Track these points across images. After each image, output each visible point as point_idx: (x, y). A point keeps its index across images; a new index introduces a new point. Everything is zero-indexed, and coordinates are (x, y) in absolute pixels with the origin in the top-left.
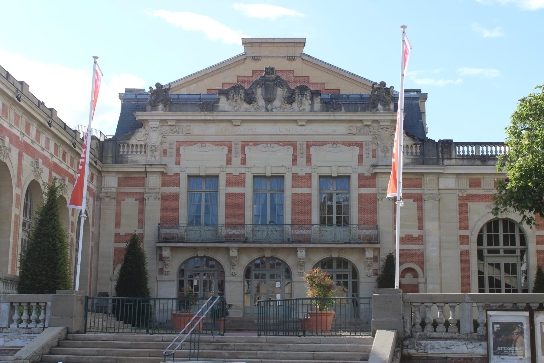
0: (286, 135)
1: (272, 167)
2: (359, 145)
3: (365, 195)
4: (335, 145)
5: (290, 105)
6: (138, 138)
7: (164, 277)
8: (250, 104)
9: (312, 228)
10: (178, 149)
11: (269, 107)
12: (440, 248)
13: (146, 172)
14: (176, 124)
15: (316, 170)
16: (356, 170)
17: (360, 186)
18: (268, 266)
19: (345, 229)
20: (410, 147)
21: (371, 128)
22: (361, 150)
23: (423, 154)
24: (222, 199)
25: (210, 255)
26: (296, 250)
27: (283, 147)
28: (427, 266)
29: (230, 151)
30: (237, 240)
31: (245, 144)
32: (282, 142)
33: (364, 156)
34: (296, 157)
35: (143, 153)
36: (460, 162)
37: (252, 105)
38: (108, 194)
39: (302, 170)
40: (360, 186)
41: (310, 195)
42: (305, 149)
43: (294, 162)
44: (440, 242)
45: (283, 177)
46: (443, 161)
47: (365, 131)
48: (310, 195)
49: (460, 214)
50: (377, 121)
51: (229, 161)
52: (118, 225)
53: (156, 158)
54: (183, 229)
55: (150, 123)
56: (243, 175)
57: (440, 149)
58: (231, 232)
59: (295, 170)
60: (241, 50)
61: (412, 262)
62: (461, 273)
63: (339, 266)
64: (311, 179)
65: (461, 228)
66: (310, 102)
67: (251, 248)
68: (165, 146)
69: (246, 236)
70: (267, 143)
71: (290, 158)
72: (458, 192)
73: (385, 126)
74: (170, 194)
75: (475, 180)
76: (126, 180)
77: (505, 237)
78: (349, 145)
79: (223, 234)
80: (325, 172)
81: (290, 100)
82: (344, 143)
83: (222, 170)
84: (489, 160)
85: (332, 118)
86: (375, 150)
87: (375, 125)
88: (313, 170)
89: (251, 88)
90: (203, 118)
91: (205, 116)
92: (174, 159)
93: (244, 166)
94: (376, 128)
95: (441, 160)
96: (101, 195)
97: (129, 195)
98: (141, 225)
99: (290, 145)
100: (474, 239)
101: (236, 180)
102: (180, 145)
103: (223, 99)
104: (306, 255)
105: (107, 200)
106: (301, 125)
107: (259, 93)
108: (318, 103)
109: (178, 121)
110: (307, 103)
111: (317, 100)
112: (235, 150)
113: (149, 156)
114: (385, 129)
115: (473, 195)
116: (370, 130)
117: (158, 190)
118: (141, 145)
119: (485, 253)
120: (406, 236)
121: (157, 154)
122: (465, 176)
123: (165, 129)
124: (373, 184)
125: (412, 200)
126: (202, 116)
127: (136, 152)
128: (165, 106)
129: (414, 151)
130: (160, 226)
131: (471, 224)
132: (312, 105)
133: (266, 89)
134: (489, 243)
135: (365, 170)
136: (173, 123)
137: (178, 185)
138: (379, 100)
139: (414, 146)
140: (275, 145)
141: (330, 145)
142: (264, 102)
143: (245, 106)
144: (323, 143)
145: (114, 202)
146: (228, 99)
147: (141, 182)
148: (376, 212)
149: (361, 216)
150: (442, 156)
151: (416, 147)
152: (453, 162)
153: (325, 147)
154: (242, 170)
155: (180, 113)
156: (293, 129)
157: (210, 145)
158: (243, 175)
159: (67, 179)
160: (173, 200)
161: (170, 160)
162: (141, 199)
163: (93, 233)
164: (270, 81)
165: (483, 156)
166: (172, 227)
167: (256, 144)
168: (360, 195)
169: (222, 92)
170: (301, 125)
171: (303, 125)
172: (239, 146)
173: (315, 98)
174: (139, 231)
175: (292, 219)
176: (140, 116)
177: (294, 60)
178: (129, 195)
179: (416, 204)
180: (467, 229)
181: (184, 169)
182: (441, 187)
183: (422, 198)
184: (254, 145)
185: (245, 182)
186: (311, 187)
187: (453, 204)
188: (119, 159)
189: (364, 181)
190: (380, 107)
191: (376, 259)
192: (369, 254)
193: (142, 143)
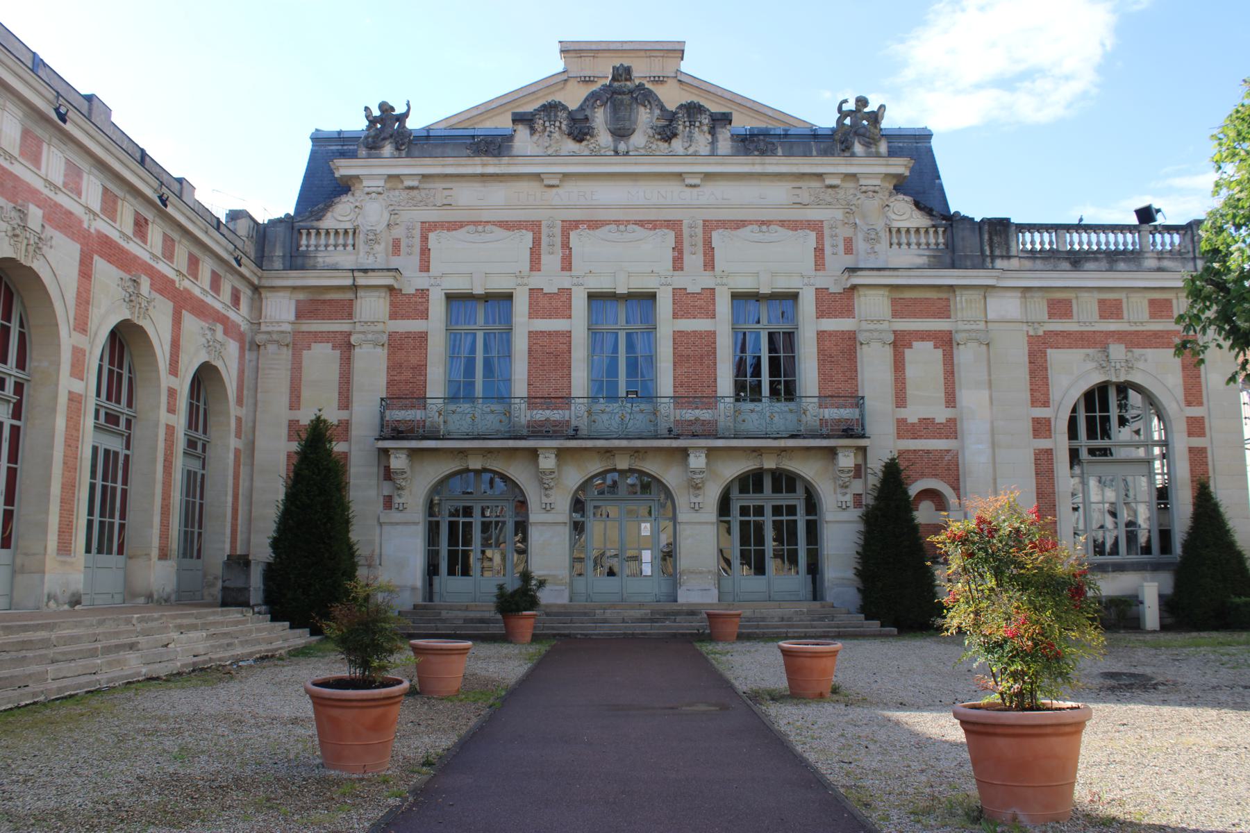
0: (659, 207)
1: (629, 275)
2: (816, 227)
3: (830, 334)
4: (764, 228)
5: (666, 145)
6: (340, 215)
7: (395, 516)
8: (581, 141)
9: (722, 406)
10: (425, 239)
11: (622, 147)
12: (994, 445)
13: (355, 288)
14: (422, 186)
15: (725, 280)
16: (812, 281)
17: (821, 314)
19: (792, 405)
20: (922, 231)
21: (841, 193)
22: (820, 238)
23: (950, 246)
24: (520, 344)
25: (497, 465)
26: (685, 452)
27: (652, 232)
28: (968, 484)
29: (537, 242)
30: (555, 432)
31: (570, 226)
32: (649, 222)
33: (828, 250)
34: (681, 252)
35: (350, 248)
36: (1028, 264)
37: (584, 143)
38: (275, 337)
39: (694, 279)
40: (821, 314)
41: (712, 334)
42: (700, 235)
43: (678, 263)
44: (993, 432)
45: (653, 296)
46: (992, 262)
47: (829, 199)
48: (712, 334)
49: (1032, 373)
50: (853, 177)
51: (535, 263)
53: (378, 256)
55: (365, 183)
56: (566, 293)
57: (986, 237)
58: (540, 415)
59: (680, 280)
60: (556, 65)
61: (935, 476)
62: (1038, 498)
63: (777, 489)
65: (1034, 402)
66: (709, 137)
67: (586, 449)
68: (398, 232)
69: (574, 423)
70: (617, 222)
71: (669, 255)
72: (1025, 327)
74: (408, 335)
75: (1059, 301)
76: (315, 305)
78: (795, 229)
79: (523, 421)
81: (667, 133)
83: (519, 281)
84: (1087, 260)
85: (758, 169)
86: (851, 239)
87: (850, 185)
88: (719, 281)
89: (581, 108)
90: (479, 170)
91: (484, 165)
92: (416, 259)
93: (567, 273)
94: (852, 191)
95: (988, 260)
96: (260, 338)
97: (318, 337)
98: (345, 402)
99: (668, 227)
100: (1062, 426)
102: (430, 230)
103: (522, 132)
104: (707, 464)
105: (271, 348)
106: (691, 186)
107: (600, 118)
108: (725, 140)
109: (424, 177)
110: (702, 140)
111: (724, 135)
112: (549, 239)
113: (362, 254)
114: (871, 194)
115: (1056, 333)
117: (380, 327)
118: (346, 232)
119: (1084, 454)
120: (921, 420)
121: (379, 248)
122: (1039, 294)
123: (399, 195)
124: (848, 312)
125: (930, 345)
126: (476, 166)
127: (336, 246)
128: (398, 149)
129: (932, 240)
130: (387, 403)
131: (1055, 394)
132: (713, 143)
133: (616, 109)
134: (1091, 435)
135: (832, 280)
136: (415, 183)
137: (424, 315)
138: (856, 134)
139: (931, 231)
141: (755, 227)
142: (610, 138)
143: (571, 145)
144: (740, 224)
145: (286, 354)
146: (533, 131)
147: (346, 310)
149: (824, 377)
150: (992, 251)
151: (936, 232)
152: (1014, 263)
153: (745, 232)
154: (565, 281)
155: (428, 161)
156: (673, 193)
158: (566, 293)
160: (414, 348)
161: (408, 262)
162: (346, 346)
163: (239, 420)
164: (624, 93)
165: (1071, 252)
166: (413, 407)
167: (594, 225)
168: (821, 335)
169: (518, 119)
170: (691, 186)
171: (695, 186)
172: (558, 231)
173: (719, 130)
174: (343, 415)
176: (344, 168)
178: (318, 337)
179: (940, 352)
180: (1046, 404)
181: (438, 281)
182: (991, 316)
183: (951, 340)
184: (589, 227)
185: (570, 308)
186: (714, 317)
187: (1019, 353)
188: (297, 260)
189: (831, 304)
190: (858, 148)
191: (858, 471)
192: (847, 461)
193: (348, 226)
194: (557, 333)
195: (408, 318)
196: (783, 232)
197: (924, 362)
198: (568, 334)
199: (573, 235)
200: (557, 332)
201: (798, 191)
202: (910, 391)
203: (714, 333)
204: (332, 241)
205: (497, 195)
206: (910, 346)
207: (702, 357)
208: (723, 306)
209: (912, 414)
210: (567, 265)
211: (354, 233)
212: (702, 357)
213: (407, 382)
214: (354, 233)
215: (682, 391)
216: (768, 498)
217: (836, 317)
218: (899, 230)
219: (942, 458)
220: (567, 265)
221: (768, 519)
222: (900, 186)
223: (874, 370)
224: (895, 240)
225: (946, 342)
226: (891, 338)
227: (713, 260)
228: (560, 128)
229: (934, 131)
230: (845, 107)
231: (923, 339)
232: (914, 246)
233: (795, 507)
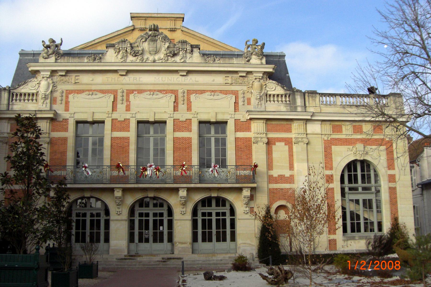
0: (168, 84)
2: (235, 93)
3: (241, 139)
4: (213, 93)
8: (136, 56)
9: (193, 169)
10: (67, 97)
17: (236, 130)
18: (151, 205)
22: (237, 98)
24: (107, 143)
32: (164, 90)
33: (240, 103)
34: (177, 104)
35: (34, 101)
37: (136, 57)
40: (236, 130)
41: (190, 138)
42: (186, 96)
43: (176, 108)
45: (165, 122)
47: (240, 82)
49: (326, 156)
54: (70, 170)
55: (42, 73)
56: (127, 121)
59: (177, 116)
63: (217, 205)
70: (150, 90)
71: (172, 105)
73: (258, 77)
74: (59, 138)
75: (337, 126)
77: (363, 176)
78: (226, 94)
80: (204, 117)
82: (221, 92)
92: (63, 106)
93: (129, 112)
99: (172, 93)
101: (120, 125)
102: (70, 93)
104: (187, 194)
111: (196, 53)
115: (336, 139)
116: (245, 80)
118: (33, 94)
119: (347, 190)
120: (279, 176)
122: (329, 123)
124: (248, 129)
125: (283, 144)
127: (28, 100)
131: (334, 165)
134: (350, 181)
136: (64, 74)
137: (66, 130)
140: (158, 93)
143: (131, 58)
144: (202, 92)
149: (238, 157)
151: (286, 96)
160: (62, 144)
161: (59, 108)
166: (60, 170)
167: (140, 92)
172: (125, 94)
175: (174, 161)
177: (174, 31)
180: (331, 169)
182: (308, 132)
184: (138, 93)
186: (191, 131)
189: (241, 126)
193: (35, 91)
194: (123, 138)
195: (60, 131)
196: (221, 96)
197: (280, 151)
199: (131, 96)
200: (123, 138)
201: (227, 78)
202: (275, 163)
203: (191, 138)
204: (27, 98)
205: (99, 78)
206: (275, 144)
207: (186, 148)
208: (195, 126)
209: (275, 173)
210: (128, 109)
211: (37, 95)
212: (186, 148)
214: (37, 95)
215: (177, 163)
216: (214, 209)
218: (270, 95)
219: (288, 192)
220: (128, 109)
221: (214, 218)
222: (270, 76)
223: (258, 155)
224: (268, 99)
225: (288, 142)
226: (266, 140)
227: (191, 107)
228: (126, 51)
229: (286, 54)
230: (248, 43)
231: (280, 141)
232: (276, 102)
233: (225, 213)
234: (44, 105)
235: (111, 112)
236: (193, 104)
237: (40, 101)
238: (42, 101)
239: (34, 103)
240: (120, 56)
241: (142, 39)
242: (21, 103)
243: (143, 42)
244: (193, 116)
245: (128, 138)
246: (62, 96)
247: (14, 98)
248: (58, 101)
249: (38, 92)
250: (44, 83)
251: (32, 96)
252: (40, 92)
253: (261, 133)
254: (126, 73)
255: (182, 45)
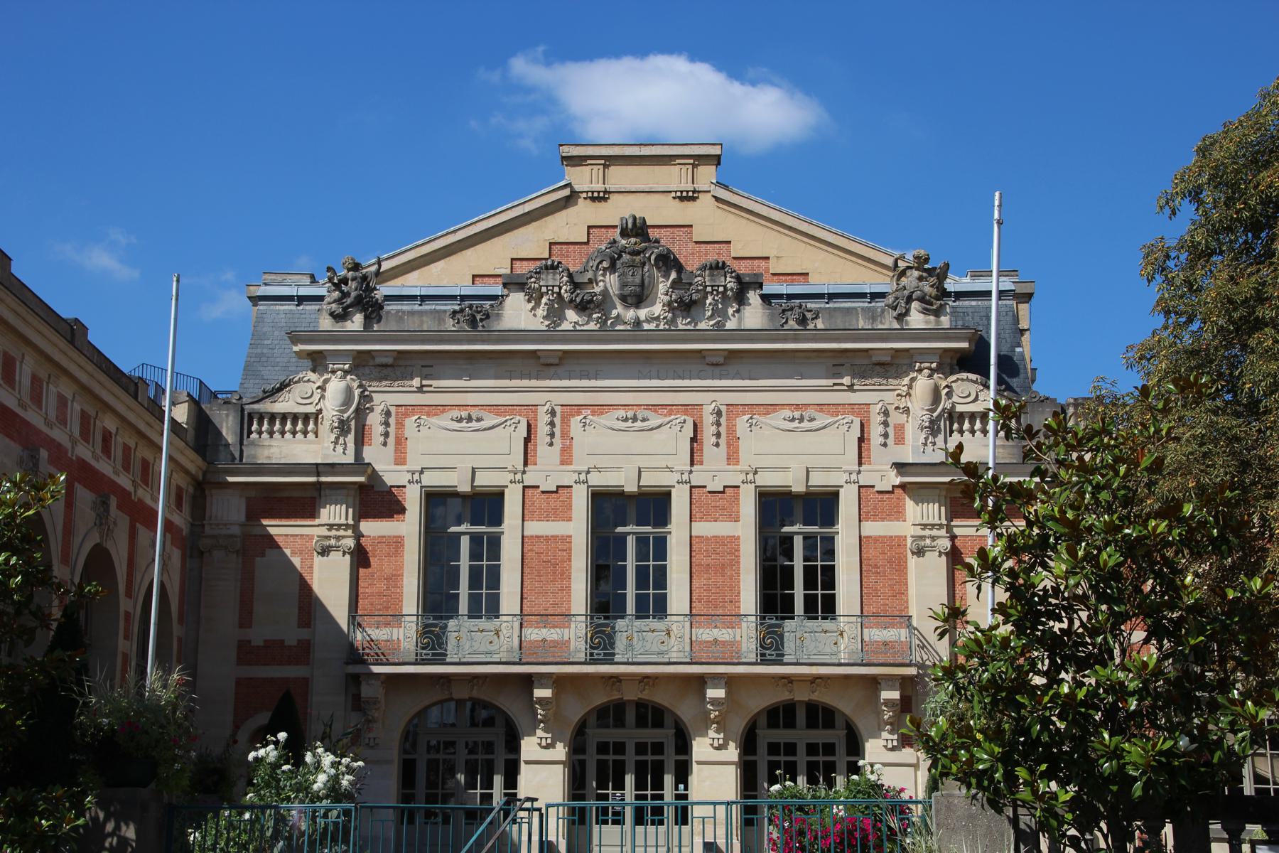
2: (861, 410)
10: (400, 425)
19: (827, 624)
52: (246, 619)
64: (738, 499)
86: (903, 426)
102: (406, 415)
111: (753, 297)
118: (306, 418)
127: (294, 433)
148: (906, 584)
157: (482, 414)
159: (113, 502)
160: (388, 555)
161: (378, 456)
163: (180, 640)
166: (387, 625)
169: (514, 283)
171: (717, 365)
174: (304, 634)
177: (693, 199)
184: (593, 413)
189: (875, 503)
198: (567, 540)
200: (555, 537)
207: (723, 567)
208: (748, 507)
211: (316, 419)
213: (380, 594)
217: (883, 519)
227: (737, 452)
234: (340, 449)
235: (521, 467)
236: (742, 445)
237: (328, 436)
238: (333, 437)
239: (311, 442)
240: (541, 311)
241: (601, 262)
242: (273, 442)
243: (605, 269)
244: (743, 477)
245: (567, 540)
246: (387, 424)
247: (255, 427)
248: (377, 437)
249: (320, 411)
250: (336, 386)
251: (305, 421)
252: (324, 412)
253: (933, 525)
254: (560, 359)
255: (711, 275)
